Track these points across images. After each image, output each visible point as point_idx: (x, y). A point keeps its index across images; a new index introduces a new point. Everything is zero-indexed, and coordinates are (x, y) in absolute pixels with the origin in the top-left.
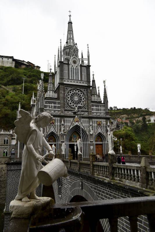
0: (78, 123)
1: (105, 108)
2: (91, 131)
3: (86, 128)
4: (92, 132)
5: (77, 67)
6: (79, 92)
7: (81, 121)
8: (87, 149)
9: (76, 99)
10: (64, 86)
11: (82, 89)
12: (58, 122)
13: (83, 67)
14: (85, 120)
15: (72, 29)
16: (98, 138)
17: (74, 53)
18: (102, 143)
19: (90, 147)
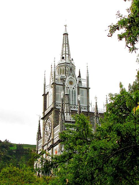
5: (74, 88)
13: (80, 89)
15: (68, 42)
17: (71, 72)
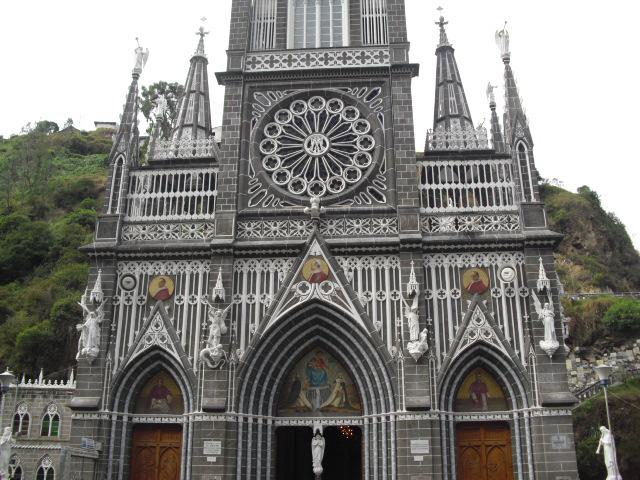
0: (326, 288)
1: (512, 184)
2: (413, 335)
3: (381, 315)
4: (423, 342)
6: (335, 106)
7: (349, 276)
8: (388, 462)
9: (317, 144)
10: (247, 85)
11: (352, 92)
12: (193, 290)
14: (373, 264)
16: (475, 384)
18: (506, 417)
19: (406, 443)
